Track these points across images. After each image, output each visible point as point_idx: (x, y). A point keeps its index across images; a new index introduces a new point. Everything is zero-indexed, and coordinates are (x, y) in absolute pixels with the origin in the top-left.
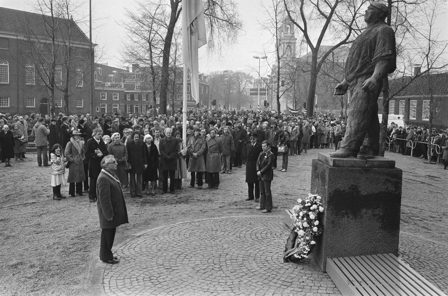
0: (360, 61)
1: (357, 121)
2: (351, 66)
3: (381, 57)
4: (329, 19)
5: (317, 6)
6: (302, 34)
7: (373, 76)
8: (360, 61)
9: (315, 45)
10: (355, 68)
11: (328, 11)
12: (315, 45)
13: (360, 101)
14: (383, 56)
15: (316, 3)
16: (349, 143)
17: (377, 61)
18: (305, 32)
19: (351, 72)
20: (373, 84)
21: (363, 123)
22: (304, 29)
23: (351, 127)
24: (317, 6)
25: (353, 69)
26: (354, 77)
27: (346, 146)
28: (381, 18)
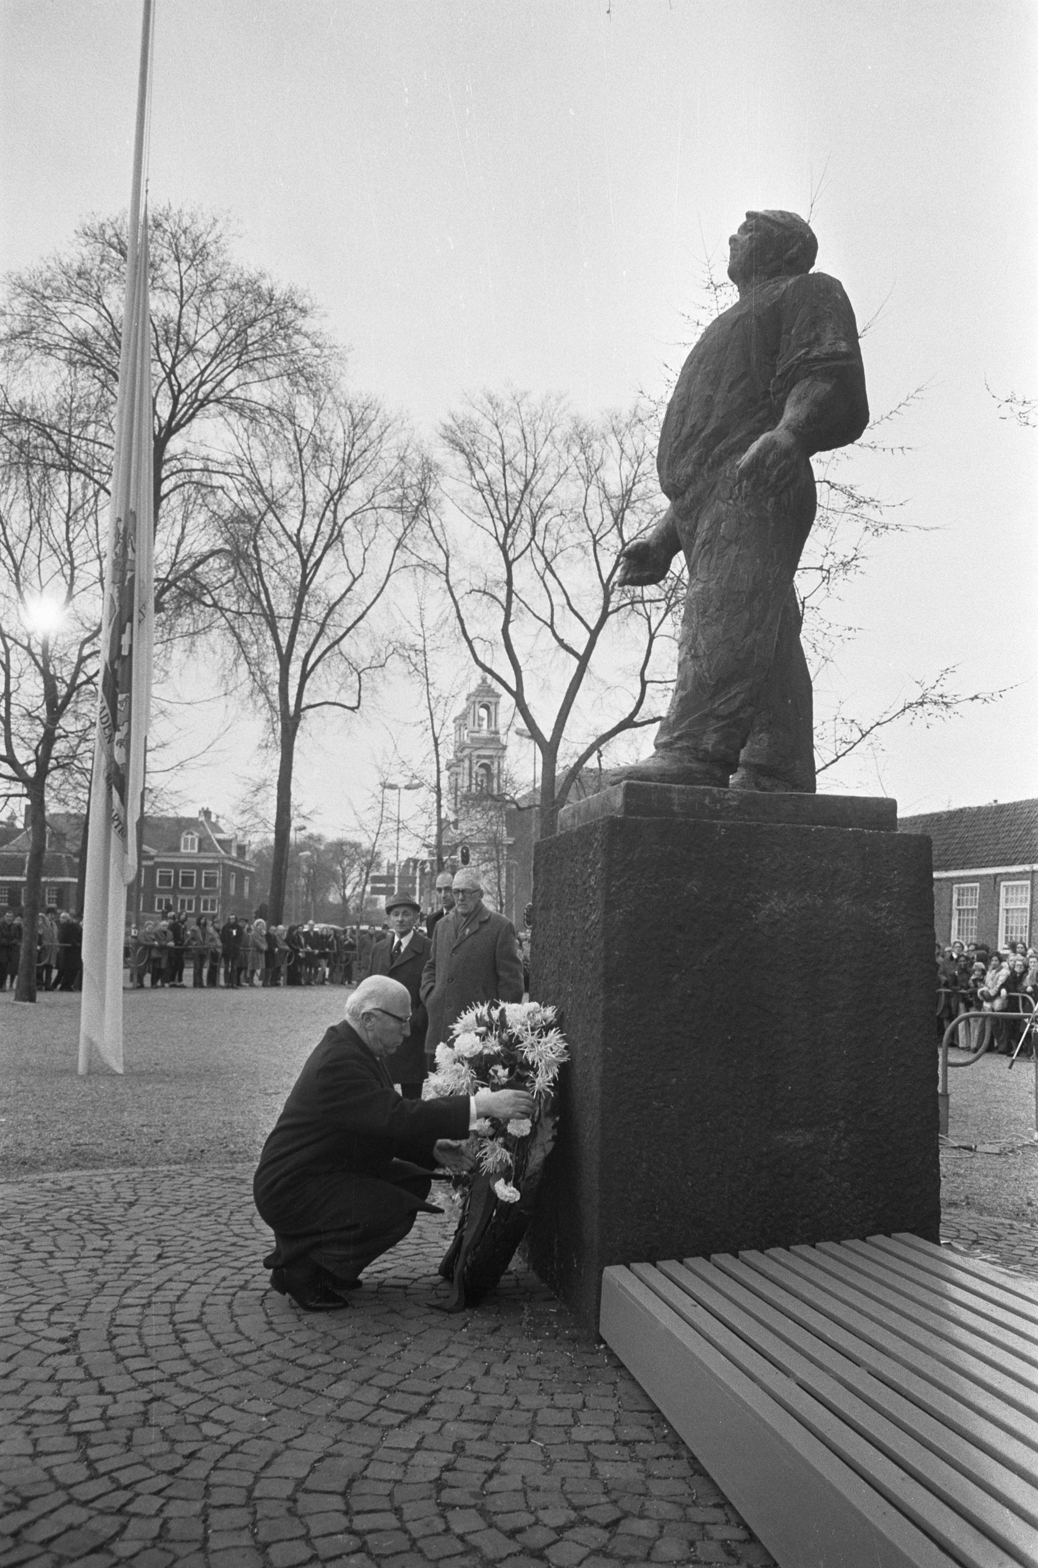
0: (719, 397)
1: (718, 629)
2: (683, 424)
3: (806, 361)
4: (584, 660)
5: (551, 626)
6: (513, 701)
7: (782, 423)
8: (719, 397)
9: (548, 736)
10: (702, 430)
11: (579, 640)
12: (548, 736)
13: (733, 552)
14: (817, 359)
15: (546, 616)
16: (689, 726)
17: (789, 381)
18: (518, 695)
19: (685, 449)
20: (787, 453)
21: (749, 640)
22: (514, 688)
23: (695, 657)
24: (551, 626)
25: (692, 436)
26: (700, 463)
27: (679, 738)
28: (791, 262)
